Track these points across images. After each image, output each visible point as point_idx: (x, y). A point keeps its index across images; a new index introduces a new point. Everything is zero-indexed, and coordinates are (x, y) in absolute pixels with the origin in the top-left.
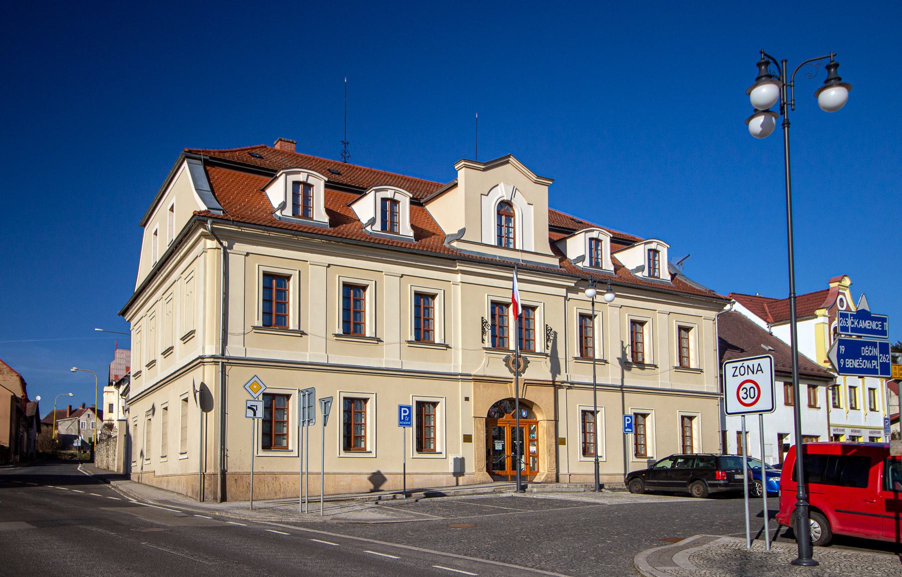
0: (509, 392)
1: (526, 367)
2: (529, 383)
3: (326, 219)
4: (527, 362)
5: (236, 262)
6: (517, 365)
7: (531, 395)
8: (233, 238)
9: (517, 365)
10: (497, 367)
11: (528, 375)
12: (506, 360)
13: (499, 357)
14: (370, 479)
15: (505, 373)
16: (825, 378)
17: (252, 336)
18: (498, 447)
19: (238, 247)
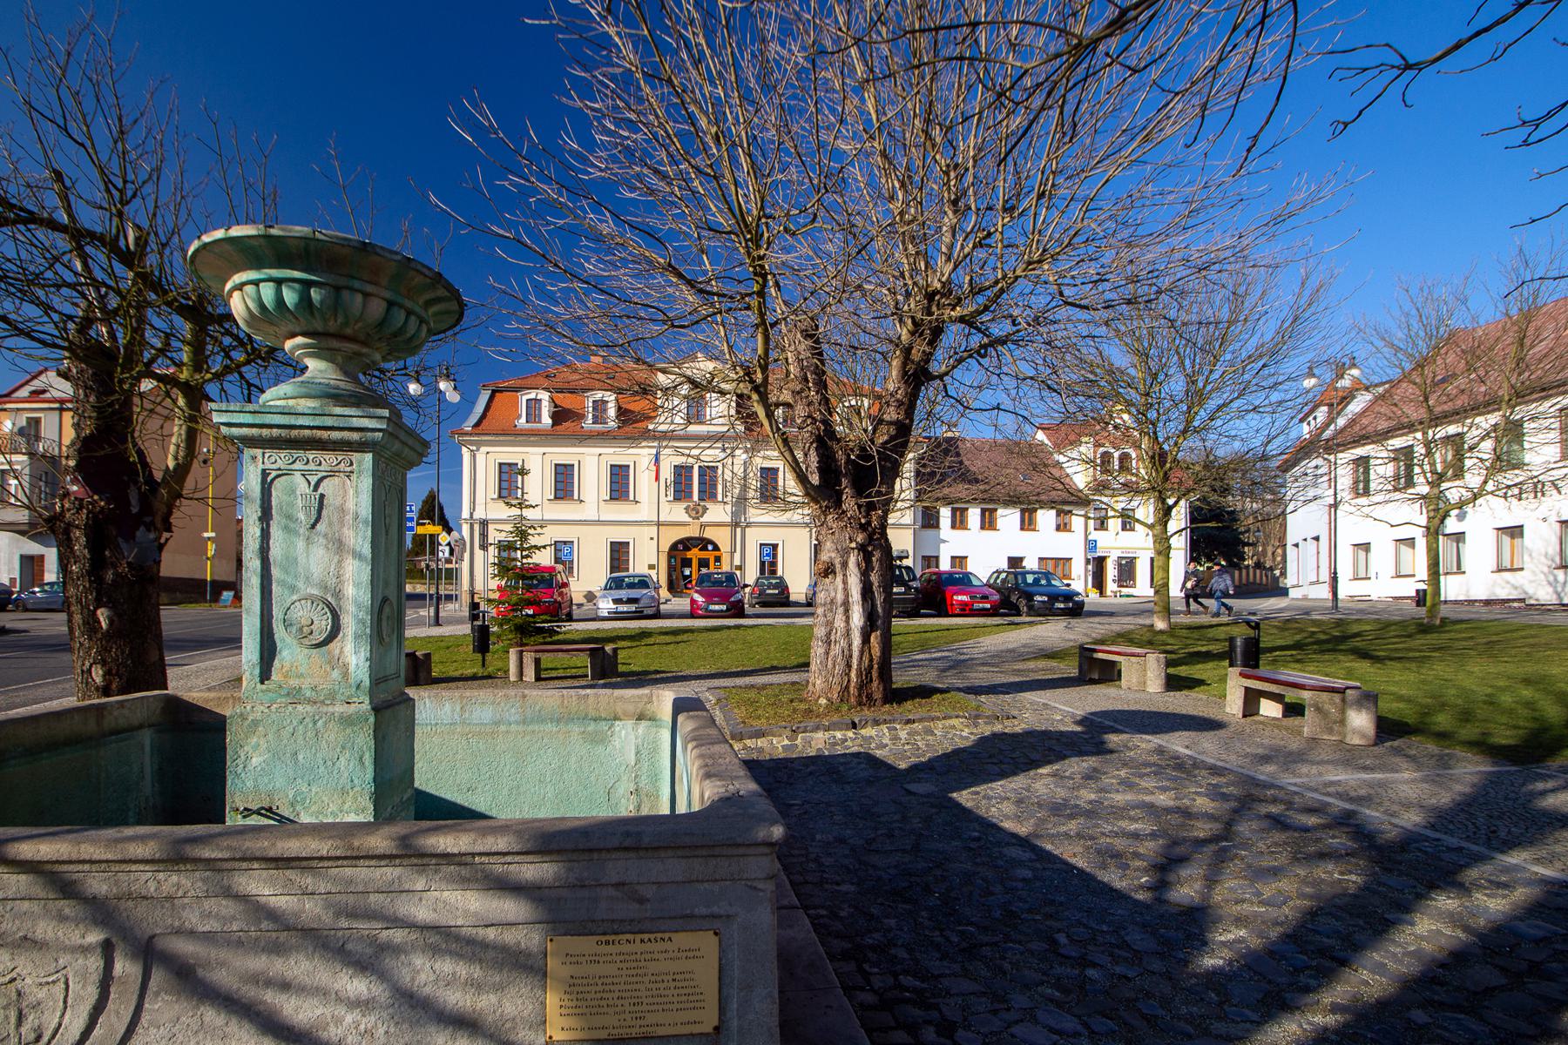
0: (692, 532)
1: (704, 512)
2: (703, 526)
3: (550, 421)
4: (705, 509)
5: (480, 457)
6: (697, 512)
7: (709, 534)
8: (479, 444)
9: (697, 512)
10: (678, 512)
11: (706, 518)
12: (687, 509)
13: (682, 506)
14: (585, 597)
15: (686, 518)
16: (1082, 501)
17: (491, 505)
18: (687, 572)
19: (484, 449)
